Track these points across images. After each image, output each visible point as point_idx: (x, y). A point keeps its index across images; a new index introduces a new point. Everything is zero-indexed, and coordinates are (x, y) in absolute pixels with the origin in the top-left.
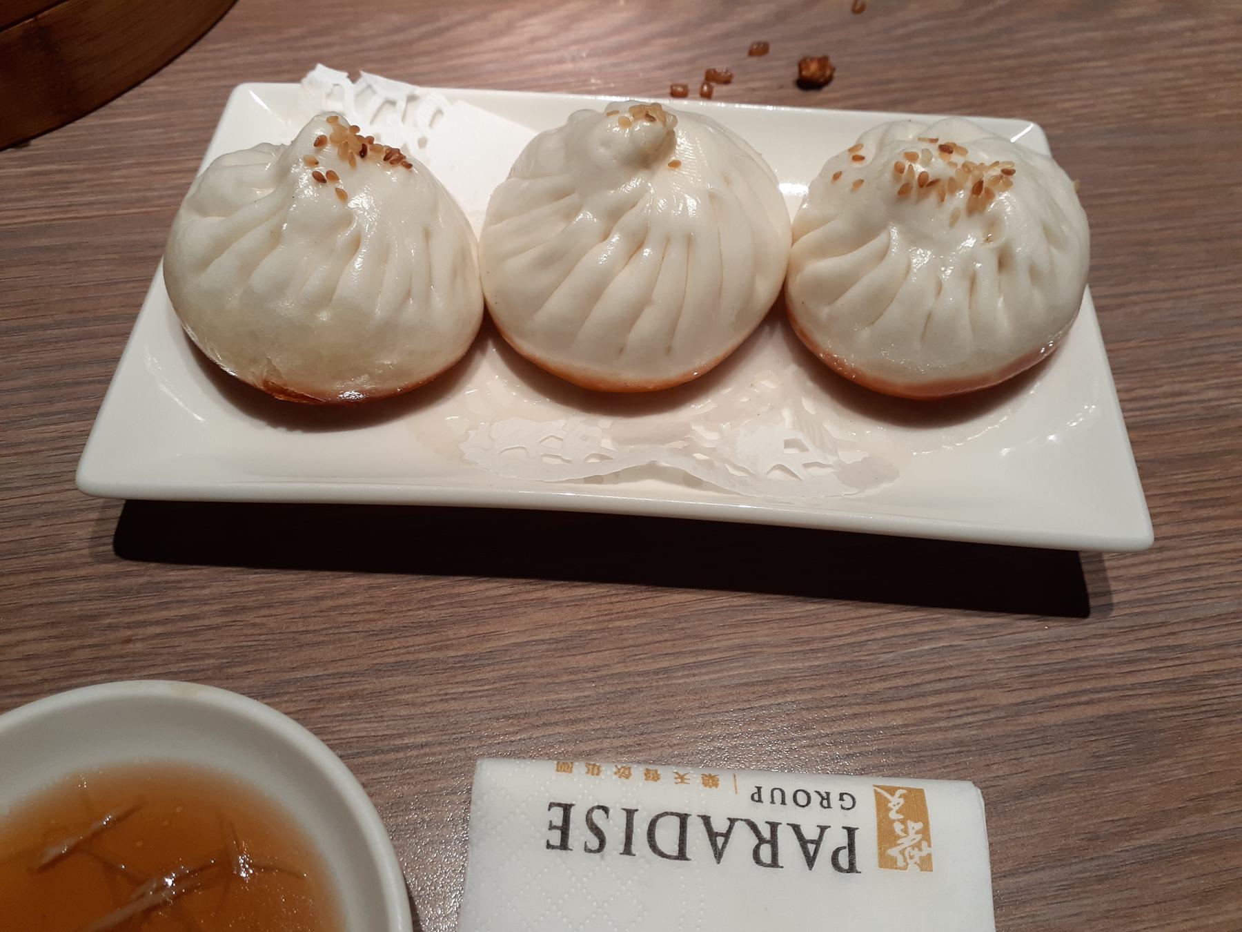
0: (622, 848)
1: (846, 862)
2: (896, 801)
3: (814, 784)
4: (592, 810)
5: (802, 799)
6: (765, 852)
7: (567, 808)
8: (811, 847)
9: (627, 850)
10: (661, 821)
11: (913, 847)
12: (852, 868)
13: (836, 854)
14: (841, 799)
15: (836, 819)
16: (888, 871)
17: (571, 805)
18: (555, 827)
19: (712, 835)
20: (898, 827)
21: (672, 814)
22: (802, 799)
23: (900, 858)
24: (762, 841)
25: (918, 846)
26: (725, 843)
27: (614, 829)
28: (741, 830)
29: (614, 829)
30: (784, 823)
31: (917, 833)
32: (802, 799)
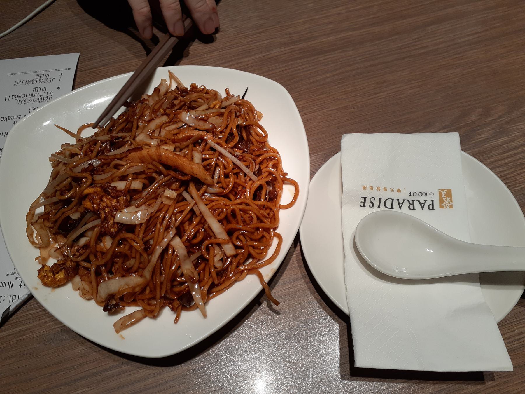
1: (431, 207)
6: (411, 207)
7: (365, 198)
8: (423, 205)
9: (379, 207)
12: (433, 209)
13: (429, 206)
19: (399, 203)
20: (444, 199)
25: (449, 203)
28: (406, 202)
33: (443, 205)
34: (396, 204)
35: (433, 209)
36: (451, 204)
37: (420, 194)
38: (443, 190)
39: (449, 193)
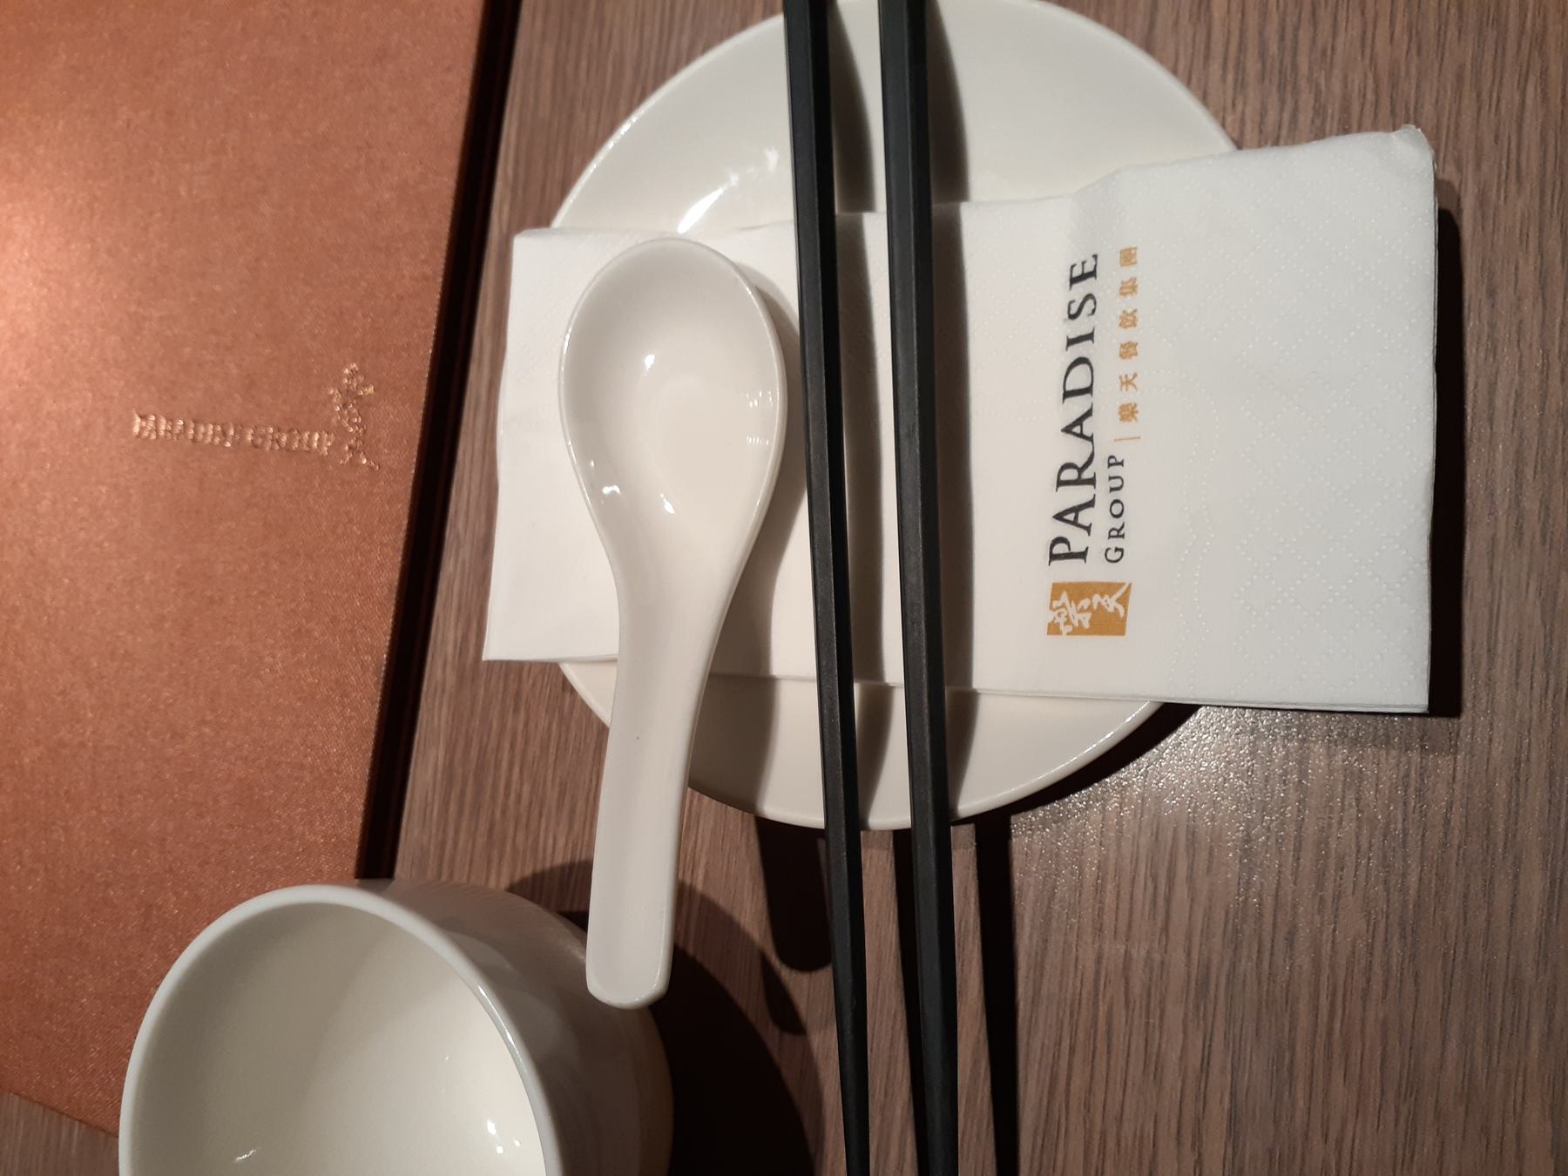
1: (1060, 552)
6: (1070, 474)
8: (1071, 517)
12: (1053, 557)
15: (1097, 543)
16: (1049, 592)
20: (1085, 603)
24: (1081, 470)
25: (1068, 622)
33: (1064, 598)
35: (1053, 557)
36: (1065, 629)
37: (1117, 509)
38: (1123, 601)
39: (1109, 624)
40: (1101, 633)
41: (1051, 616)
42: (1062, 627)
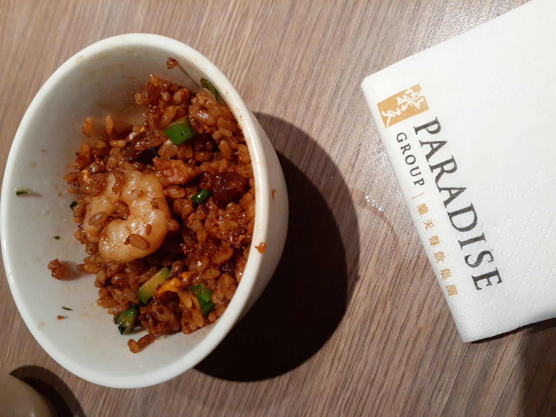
0: (482, 242)
1: (434, 126)
2: (390, 114)
3: (398, 158)
4: (470, 265)
5: (411, 160)
7: (476, 279)
8: (435, 146)
9: (482, 238)
10: (458, 226)
11: (411, 97)
12: (436, 122)
14: (402, 140)
15: (414, 139)
17: (473, 278)
18: (489, 282)
19: (453, 197)
20: (404, 108)
21: (452, 222)
22: (411, 160)
23: (419, 101)
24: (443, 171)
25: (409, 95)
26: (453, 189)
27: (475, 250)
28: (442, 184)
29: (475, 250)
30: (428, 164)
31: (403, 98)
32: (411, 160)
34: (457, 204)
40: (389, 99)
41: (422, 93)
42: (412, 91)
